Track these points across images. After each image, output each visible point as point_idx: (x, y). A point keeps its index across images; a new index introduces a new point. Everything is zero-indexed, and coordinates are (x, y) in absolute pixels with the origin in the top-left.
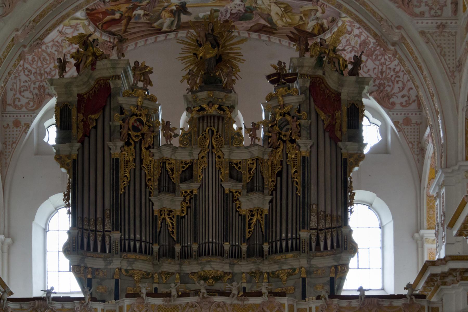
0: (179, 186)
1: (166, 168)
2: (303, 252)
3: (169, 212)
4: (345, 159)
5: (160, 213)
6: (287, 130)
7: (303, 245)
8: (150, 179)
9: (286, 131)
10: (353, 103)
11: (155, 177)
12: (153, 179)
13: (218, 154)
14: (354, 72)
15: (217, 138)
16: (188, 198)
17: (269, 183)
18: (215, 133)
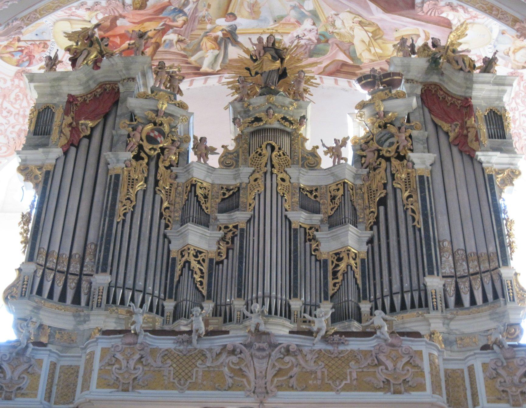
0: (216, 219)
1: (195, 192)
2: (434, 309)
3: (196, 253)
4: (491, 178)
5: (181, 254)
6: (392, 144)
7: (432, 299)
8: (167, 208)
9: (389, 146)
10: (491, 110)
11: (177, 206)
12: (173, 207)
13: (280, 176)
15: (280, 156)
16: (230, 235)
18: (277, 148)
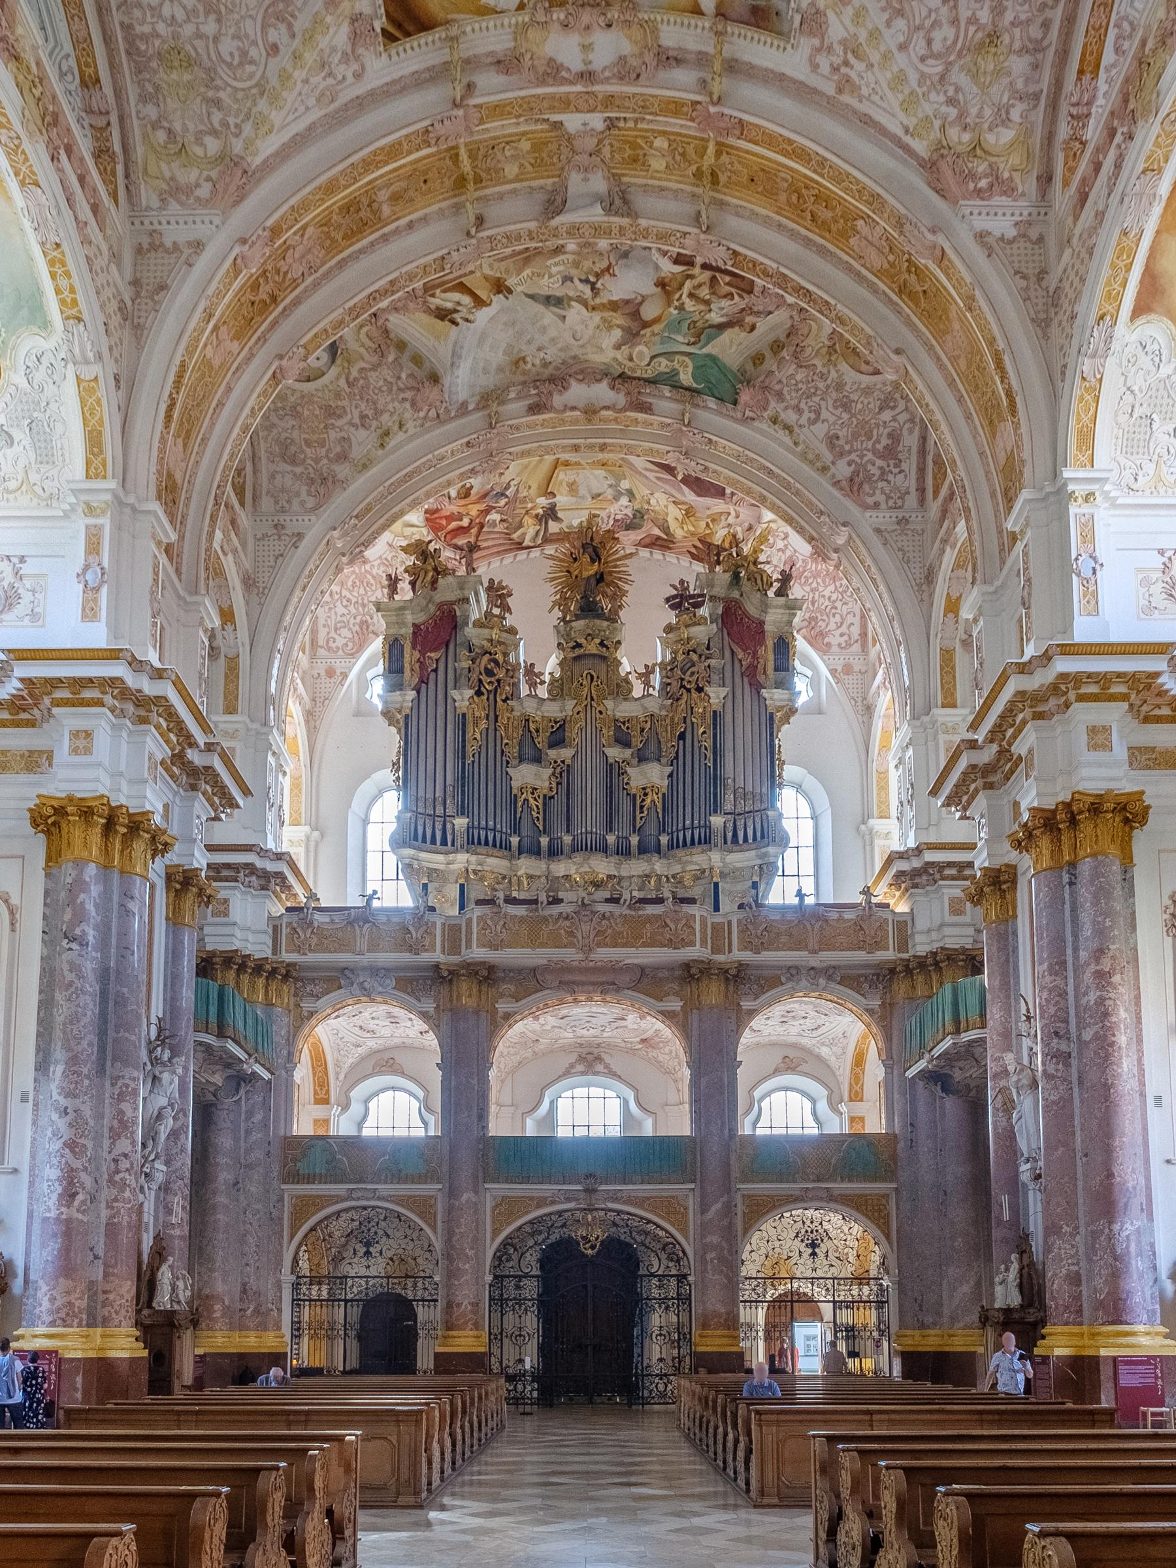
4: (772, 714)
6: (693, 674)
14: (781, 593)
17: (669, 746)
